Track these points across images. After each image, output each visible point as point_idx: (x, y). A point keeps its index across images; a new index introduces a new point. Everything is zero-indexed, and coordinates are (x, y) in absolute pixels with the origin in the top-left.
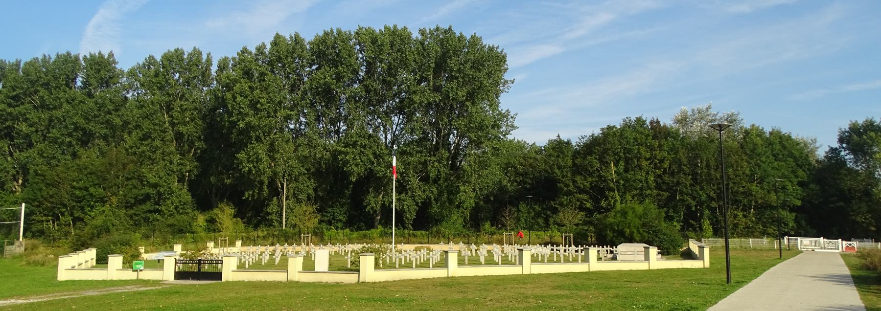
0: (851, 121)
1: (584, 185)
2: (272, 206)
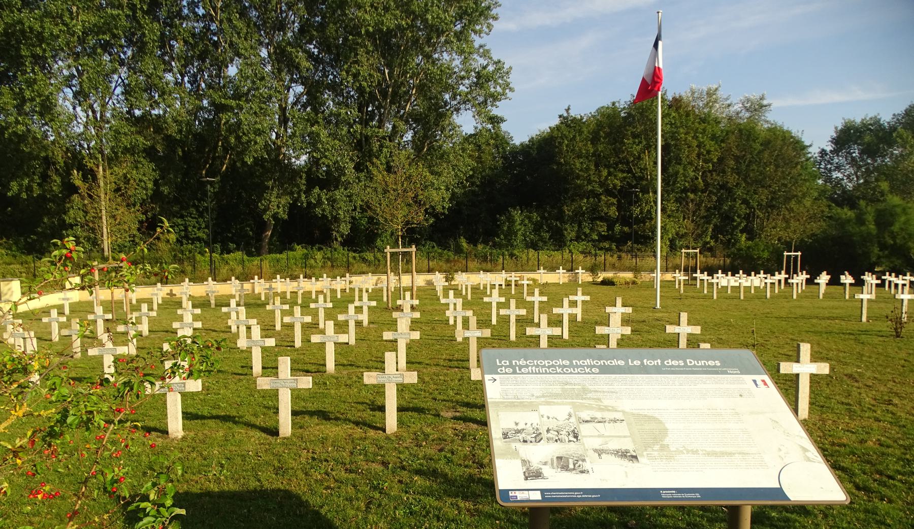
0: (843, 119)
1: (615, 186)
2: (71, 212)
